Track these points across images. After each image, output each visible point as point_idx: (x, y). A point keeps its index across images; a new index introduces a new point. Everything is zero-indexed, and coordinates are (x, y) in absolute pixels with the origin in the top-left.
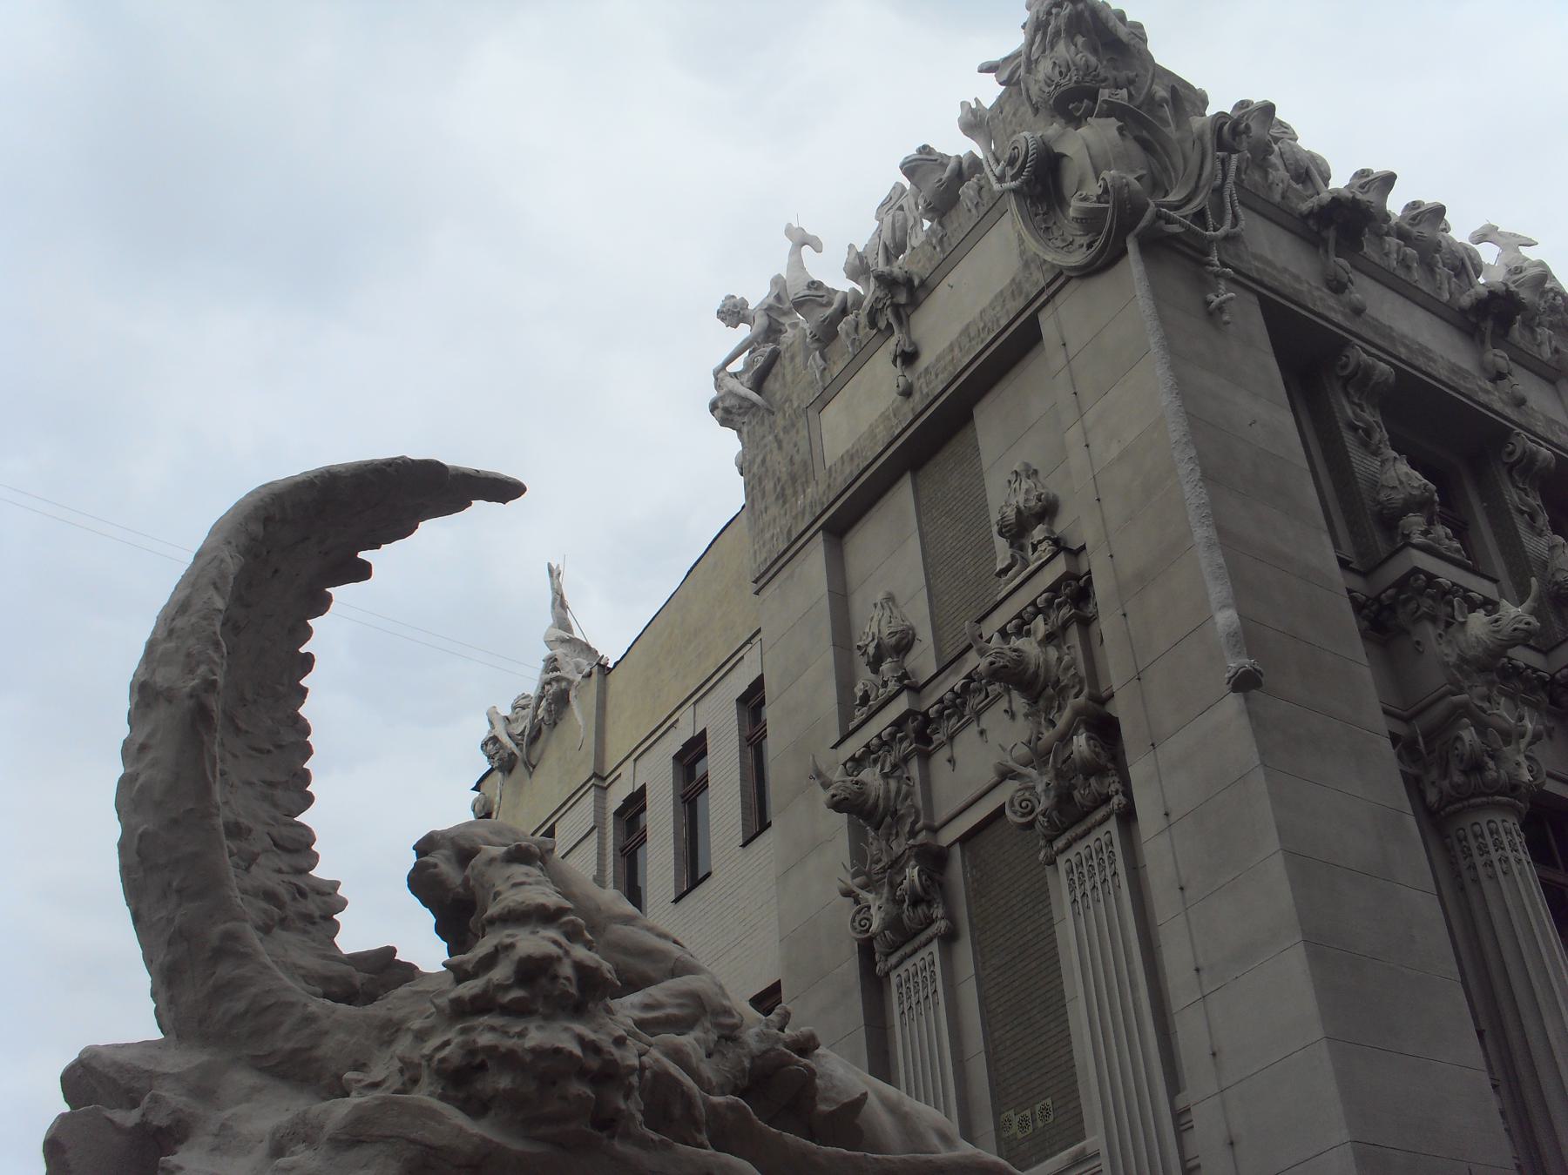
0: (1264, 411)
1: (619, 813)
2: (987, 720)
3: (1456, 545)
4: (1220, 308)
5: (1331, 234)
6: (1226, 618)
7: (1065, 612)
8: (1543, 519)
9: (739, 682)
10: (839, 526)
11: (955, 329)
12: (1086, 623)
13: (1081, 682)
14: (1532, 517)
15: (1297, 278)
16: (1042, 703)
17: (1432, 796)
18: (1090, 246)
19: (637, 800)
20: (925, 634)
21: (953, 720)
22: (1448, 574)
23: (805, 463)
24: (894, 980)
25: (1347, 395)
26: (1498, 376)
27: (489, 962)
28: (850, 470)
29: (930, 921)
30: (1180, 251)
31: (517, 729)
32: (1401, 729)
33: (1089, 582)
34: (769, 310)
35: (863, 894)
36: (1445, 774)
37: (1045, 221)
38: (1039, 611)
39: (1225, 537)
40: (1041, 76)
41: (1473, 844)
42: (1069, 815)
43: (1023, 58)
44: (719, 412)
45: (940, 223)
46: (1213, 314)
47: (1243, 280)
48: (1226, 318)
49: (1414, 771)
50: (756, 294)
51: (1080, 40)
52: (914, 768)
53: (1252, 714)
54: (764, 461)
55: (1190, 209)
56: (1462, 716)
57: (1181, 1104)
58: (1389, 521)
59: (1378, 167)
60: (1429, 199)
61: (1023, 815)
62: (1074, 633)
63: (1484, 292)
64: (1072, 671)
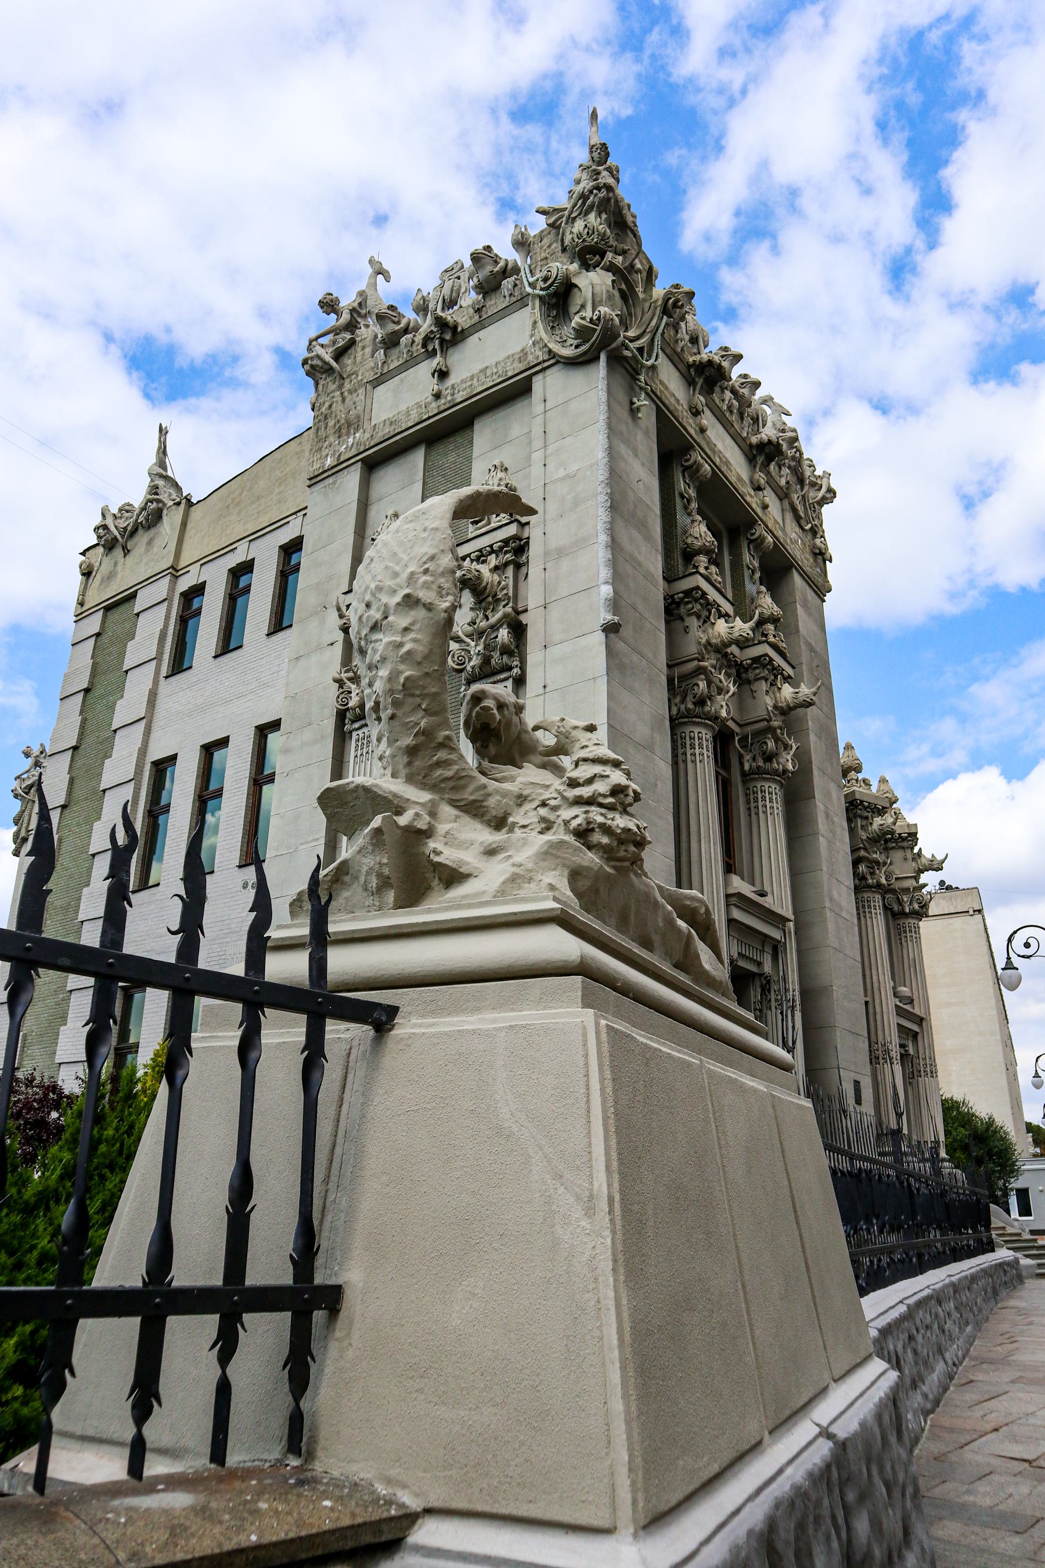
3: (719, 579)
4: (638, 409)
5: (700, 381)
6: (606, 590)
7: (509, 557)
8: (758, 575)
9: (285, 536)
10: (373, 463)
11: (476, 368)
12: (518, 566)
13: (509, 599)
15: (678, 401)
16: (483, 604)
18: (577, 347)
19: (198, 590)
22: (713, 595)
23: (358, 417)
24: (354, 734)
25: (684, 476)
26: (758, 488)
27: (590, 781)
28: (388, 430)
30: (627, 369)
31: (122, 524)
33: (527, 543)
34: (353, 311)
35: (349, 684)
36: (683, 701)
37: (553, 322)
38: (493, 552)
39: (614, 545)
40: (575, 230)
41: (688, 743)
43: (566, 213)
44: (307, 367)
45: (484, 298)
46: (634, 411)
47: (653, 396)
48: (640, 415)
51: (604, 216)
53: (608, 647)
54: (330, 406)
56: (700, 674)
58: (689, 555)
59: (735, 350)
60: (754, 376)
61: (458, 664)
62: (510, 571)
63: (765, 438)
64: (505, 591)
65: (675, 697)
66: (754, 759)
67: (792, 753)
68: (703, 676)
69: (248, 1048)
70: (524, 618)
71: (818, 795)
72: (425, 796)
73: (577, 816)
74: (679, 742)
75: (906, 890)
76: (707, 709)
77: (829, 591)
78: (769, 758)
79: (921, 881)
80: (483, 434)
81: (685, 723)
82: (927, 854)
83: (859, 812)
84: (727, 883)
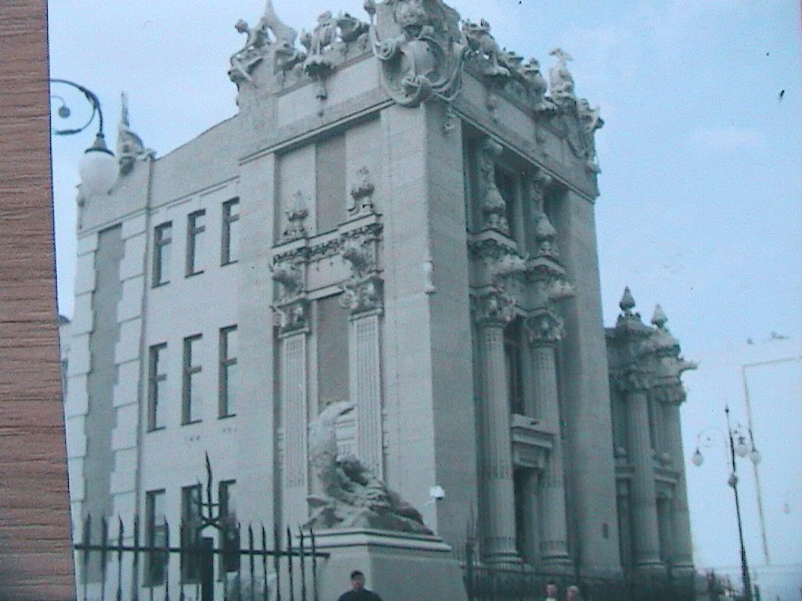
0: (455, 176)
1: (156, 228)
2: (333, 259)
6: (427, 267)
7: (372, 236)
10: (281, 154)
12: (378, 241)
14: (537, 203)
20: (312, 213)
28: (289, 134)
29: (302, 327)
32: (474, 293)
36: (484, 311)
38: (362, 233)
42: (362, 309)
46: (446, 134)
49: (474, 308)
50: (254, 25)
52: (303, 267)
55: (444, 89)
57: (385, 411)
58: (487, 213)
59: (518, 54)
62: (373, 243)
67: (561, 327)
68: (494, 298)
70: (382, 276)
72: (332, 499)
73: (369, 503)
77: (598, 195)
78: (545, 333)
80: (353, 142)
82: (688, 360)
84: (511, 419)
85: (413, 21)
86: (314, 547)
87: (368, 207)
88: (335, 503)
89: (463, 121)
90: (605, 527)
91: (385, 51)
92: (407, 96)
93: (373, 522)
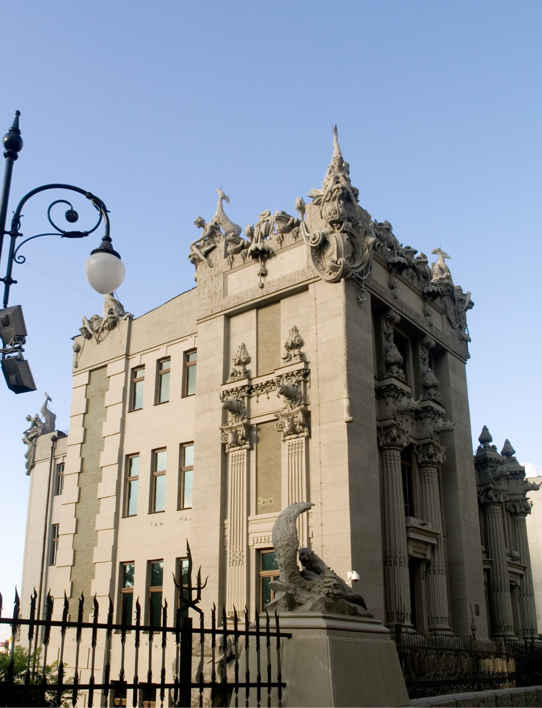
12: (306, 382)
17: (381, 444)
21: (260, 391)
22: (400, 385)
27: (329, 582)
33: (309, 372)
36: (386, 438)
37: (318, 258)
38: (293, 375)
41: (388, 458)
43: (323, 198)
49: (379, 436)
65: (381, 435)
66: (424, 456)
67: (443, 453)
69: (268, 644)
70: (309, 408)
71: (458, 469)
72: (293, 586)
73: (326, 590)
74: (384, 457)
75: (518, 501)
76: (397, 442)
79: (527, 496)
81: (387, 449)
83: (489, 464)
85: (337, 217)
86: (278, 627)
87: (298, 356)
88: (295, 589)
89: (372, 295)
90: (477, 606)
91: (314, 239)
92: (330, 274)
93: (328, 607)
